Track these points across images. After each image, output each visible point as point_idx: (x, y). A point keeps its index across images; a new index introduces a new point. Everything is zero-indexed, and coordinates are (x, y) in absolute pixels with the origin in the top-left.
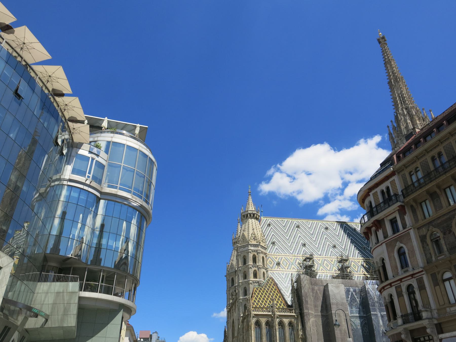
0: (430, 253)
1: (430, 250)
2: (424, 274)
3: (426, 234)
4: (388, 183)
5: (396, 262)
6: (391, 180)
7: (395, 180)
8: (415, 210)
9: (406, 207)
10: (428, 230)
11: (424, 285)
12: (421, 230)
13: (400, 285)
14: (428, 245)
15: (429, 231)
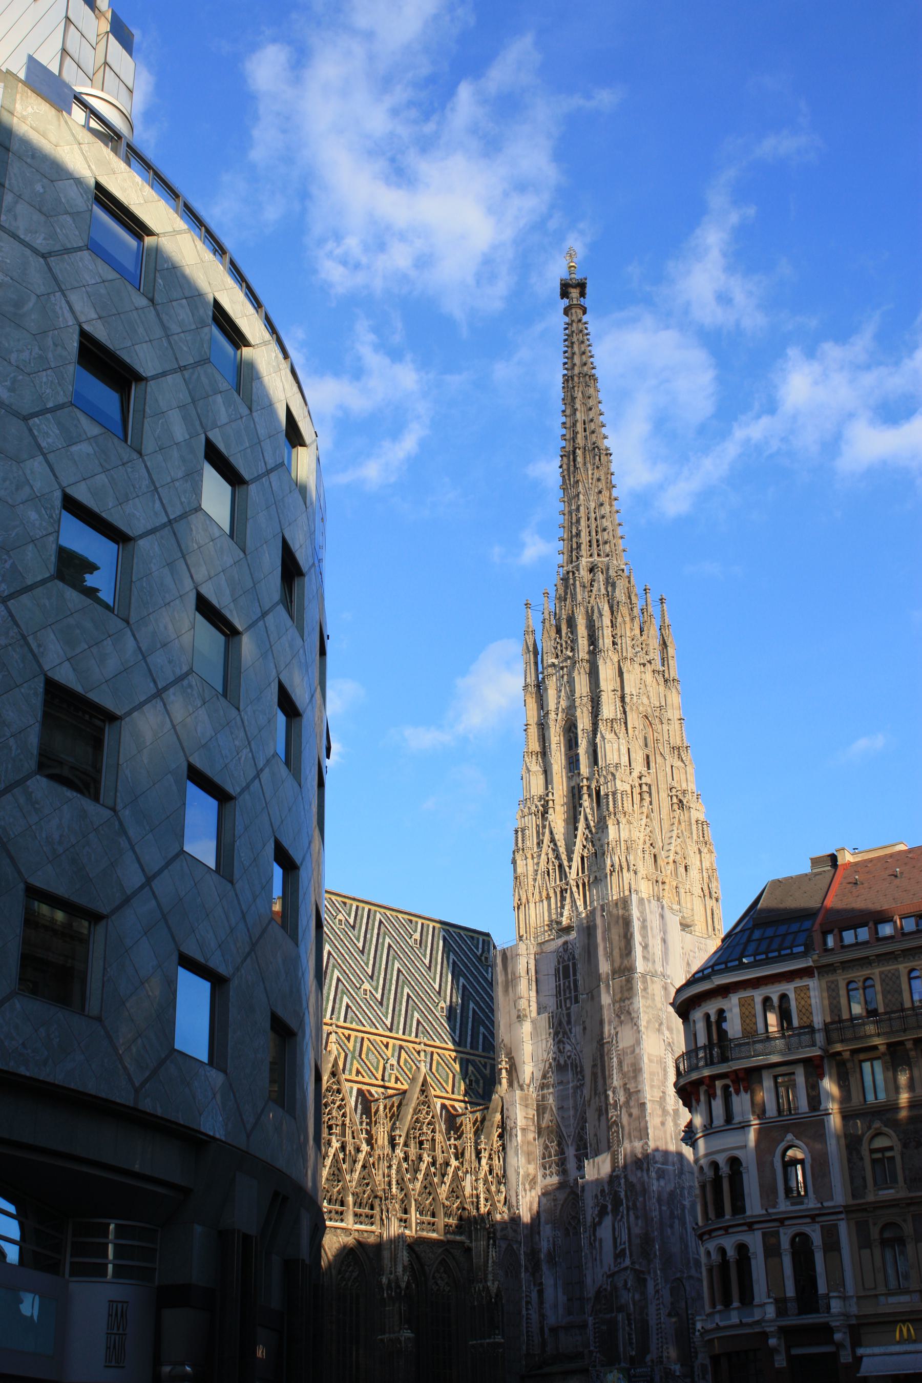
0: (864, 1178)
1: (864, 1170)
2: (843, 1219)
3: (863, 1134)
4: (789, 988)
5: (775, 1179)
6: (799, 983)
7: (809, 989)
8: (847, 1073)
9: (826, 1061)
10: (869, 1128)
11: (838, 1242)
12: (851, 1122)
13: (778, 1233)
14: (862, 1159)
15: (871, 1131)
